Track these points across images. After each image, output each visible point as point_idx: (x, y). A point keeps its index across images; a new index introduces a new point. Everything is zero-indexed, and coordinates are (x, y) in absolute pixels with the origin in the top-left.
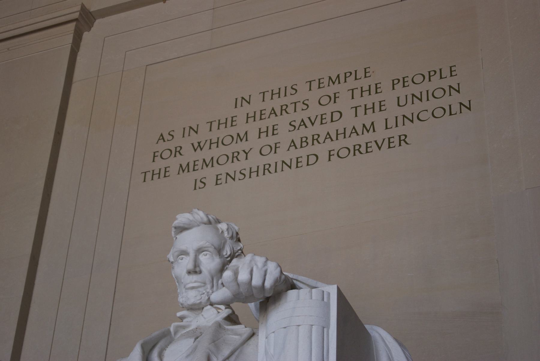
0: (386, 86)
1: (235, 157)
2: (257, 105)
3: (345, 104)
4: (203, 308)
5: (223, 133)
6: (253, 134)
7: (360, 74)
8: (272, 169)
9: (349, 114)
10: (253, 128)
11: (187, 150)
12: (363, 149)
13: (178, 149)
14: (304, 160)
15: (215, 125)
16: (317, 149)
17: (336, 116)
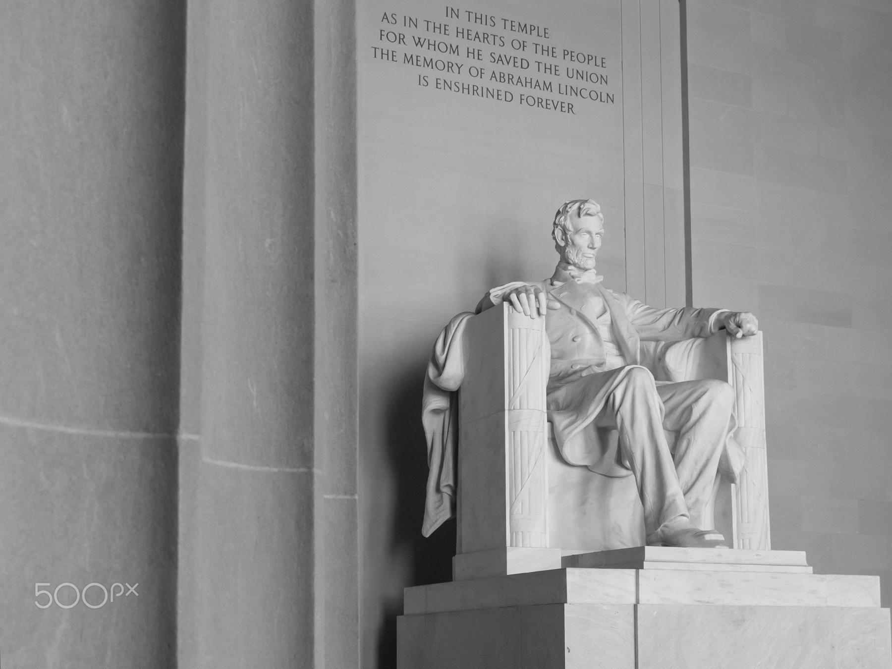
0: (559, 52)
1: (449, 66)
2: (463, 23)
3: (529, 54)
4: (586, 270)
5: (436, 37)
6: (463, 51)
7: (542, 33)
8: (479, 91)
9: (533, 66)
10: (463, 44)
11: (408, 39)
12: (544, 103)
13: (402, 37)
14: (503, 93)
15: (431, 26)
16: (511, 88)
17: (525, 64)
